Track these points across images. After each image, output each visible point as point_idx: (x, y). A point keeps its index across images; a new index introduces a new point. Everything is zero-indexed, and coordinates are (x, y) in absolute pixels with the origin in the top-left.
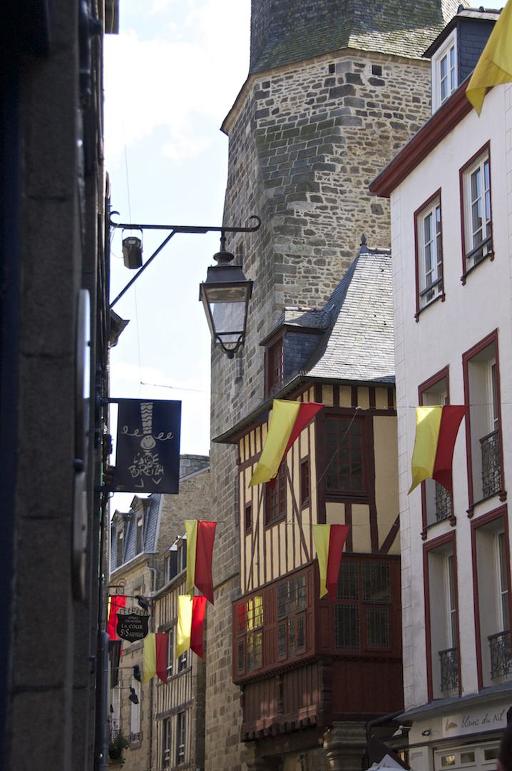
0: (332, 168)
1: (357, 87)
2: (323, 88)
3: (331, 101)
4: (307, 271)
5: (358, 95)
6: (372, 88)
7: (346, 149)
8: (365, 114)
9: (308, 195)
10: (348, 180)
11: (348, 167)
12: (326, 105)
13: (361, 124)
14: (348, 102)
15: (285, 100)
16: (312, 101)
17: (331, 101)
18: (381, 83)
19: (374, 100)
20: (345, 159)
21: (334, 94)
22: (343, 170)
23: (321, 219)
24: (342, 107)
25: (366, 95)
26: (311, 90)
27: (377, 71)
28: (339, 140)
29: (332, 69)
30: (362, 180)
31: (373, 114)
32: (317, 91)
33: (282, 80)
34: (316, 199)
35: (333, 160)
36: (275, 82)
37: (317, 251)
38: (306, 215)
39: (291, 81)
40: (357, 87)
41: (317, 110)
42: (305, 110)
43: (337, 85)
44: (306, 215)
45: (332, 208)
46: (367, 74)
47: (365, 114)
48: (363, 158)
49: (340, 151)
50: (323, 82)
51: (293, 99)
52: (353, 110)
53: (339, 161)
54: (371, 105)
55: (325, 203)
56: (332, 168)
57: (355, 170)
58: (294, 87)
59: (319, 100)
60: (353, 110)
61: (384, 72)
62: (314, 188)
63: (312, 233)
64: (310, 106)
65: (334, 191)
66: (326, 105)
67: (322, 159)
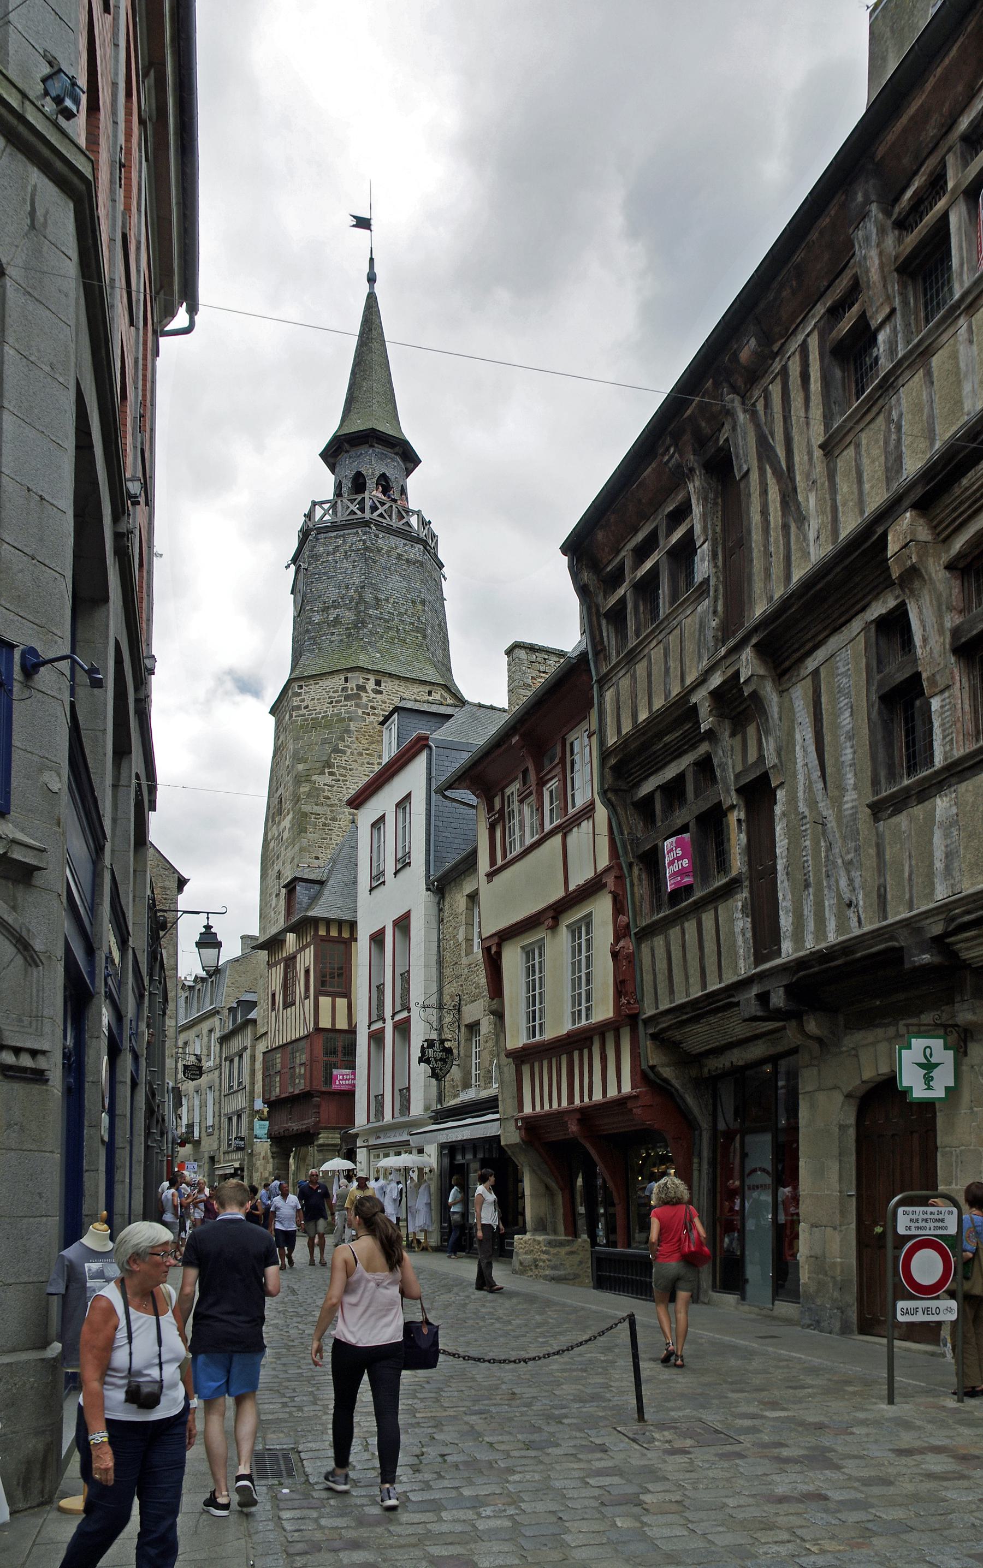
0: (344, 752)
1: (363, 694)
4: (324, 825)
5: (364, 700)
6: (374, 696)
7: (354, 739)
8: (368, 714)
9: (326, 771)
10: (356, 761)
11: (356, 752)
13: (365, 721)
14: (357, 705)
16: (332, 702)
18: (381, 693)
19: (375, 705)
20: (354, 746)
21: (347, 698)
22: (352, 754)
23: (335, 788)
24: (353, 708)
25: (370, 701)
26: (331, 694)
27: (378, 683)
28: (348, 731)
29: (346, 680)
30: (365, 761)
31: (374, 714)
34: (331, 774)
35: (345, 746)
36: (306, 686)
37: (332, 811)
38: (325, 785)
39: (317, 686)
40: (363, 694)
43: (350, 692)
44: (325, 785)
45: (343, 781)
46: (371, 685)
47: (368, 714)
48: (366, 746)
49: (350, 740)
51: (318, 699)
52: (360, 711)
53: (349, 747)
54: (373, 708)
55: (338, 777)
56: (344, 752)
57: (361, 754)
59: (336, 702)
60: (360, 711)
61: (383, 685)
62: (329, 764)
63: (329, 798)
65: (345, 768)
67: (337, 744)
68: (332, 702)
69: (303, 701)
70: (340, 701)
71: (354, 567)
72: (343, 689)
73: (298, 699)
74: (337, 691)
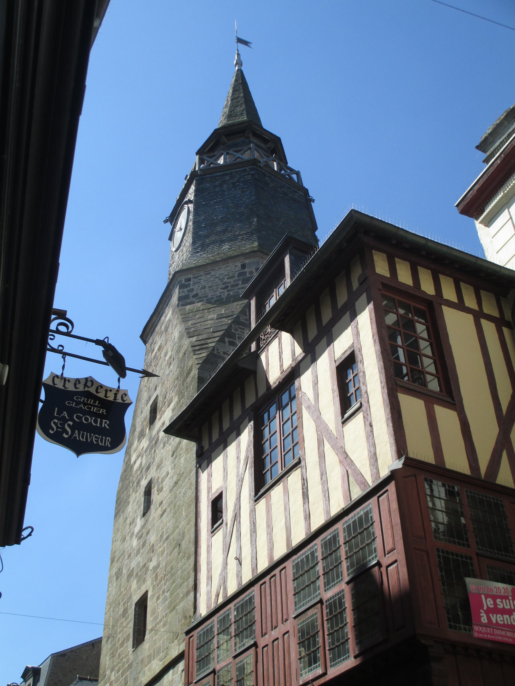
2: (236, 278)
3: (243, 286)
12: (239, 289)
15: (204, 288)
16: (227, 287)
17: (243, 286)
26: (225, 280)
32: (232, 280)
33: (201, 276)
36: (195, 278)
39: (209, 276)
41: (231, 293)
42: (221, 293)
50: (236, 275)
51: (209, 287)
58: (212, 279)
59: (232, 286)
64: (225, 291)
66: (239, 289)
68: (227, 287)
69: (192, 290)
70: (237, 285)
71: (243, 192)
72: (240, 275)
73: (185, 290)
74: (233, 277)
